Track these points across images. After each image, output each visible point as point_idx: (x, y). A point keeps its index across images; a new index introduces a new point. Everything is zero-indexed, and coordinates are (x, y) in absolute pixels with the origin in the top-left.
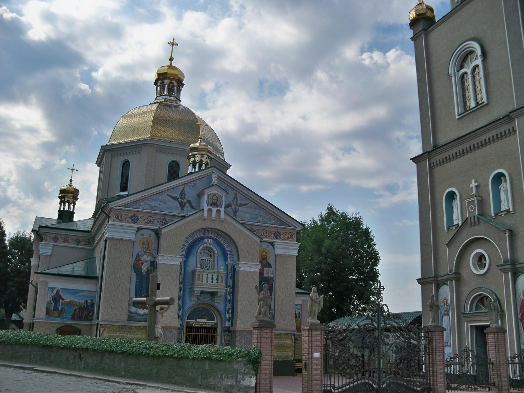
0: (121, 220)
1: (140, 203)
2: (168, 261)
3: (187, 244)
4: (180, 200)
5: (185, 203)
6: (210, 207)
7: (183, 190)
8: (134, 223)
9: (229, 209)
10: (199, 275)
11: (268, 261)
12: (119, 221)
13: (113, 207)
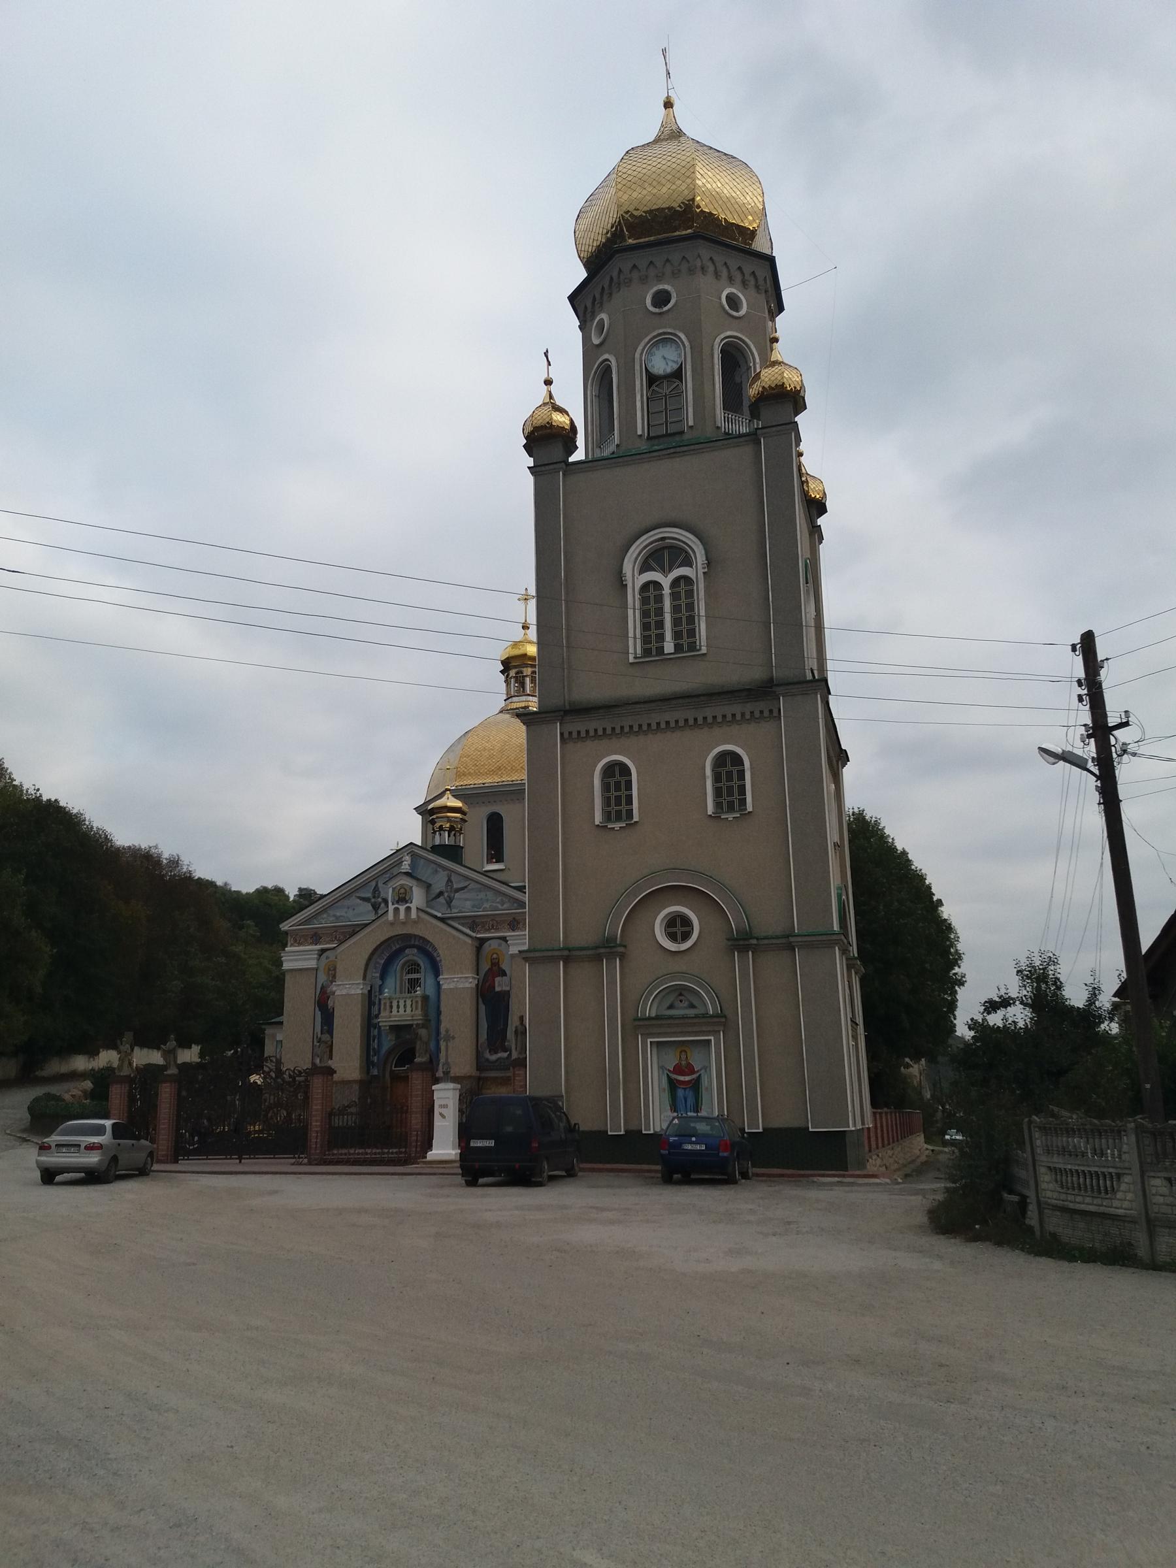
0: (300, 944)
1: (322, 916)
2: (345, 991)
3: (382, 962)
4: (373, 900)
5: (380, 904)
6: (396, 906)
7: (377, 885)
8: (316, 944)
9: (441, 900)
10: (385, 1004)
11: (501, 966)
12: (297, 945)
13: (286, 928)
